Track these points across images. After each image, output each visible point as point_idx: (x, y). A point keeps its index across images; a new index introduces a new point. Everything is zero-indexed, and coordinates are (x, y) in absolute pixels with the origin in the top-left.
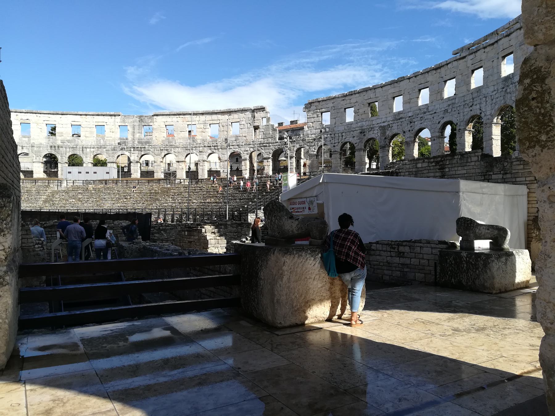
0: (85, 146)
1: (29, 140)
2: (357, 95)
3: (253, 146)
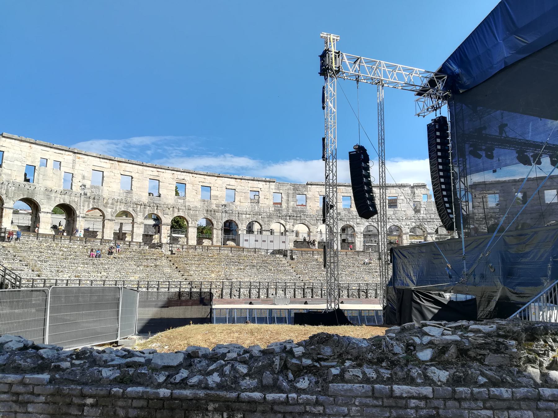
0: (241, 212)
1: (185, 202)
2: (531, 182)
3: (415, 221)
